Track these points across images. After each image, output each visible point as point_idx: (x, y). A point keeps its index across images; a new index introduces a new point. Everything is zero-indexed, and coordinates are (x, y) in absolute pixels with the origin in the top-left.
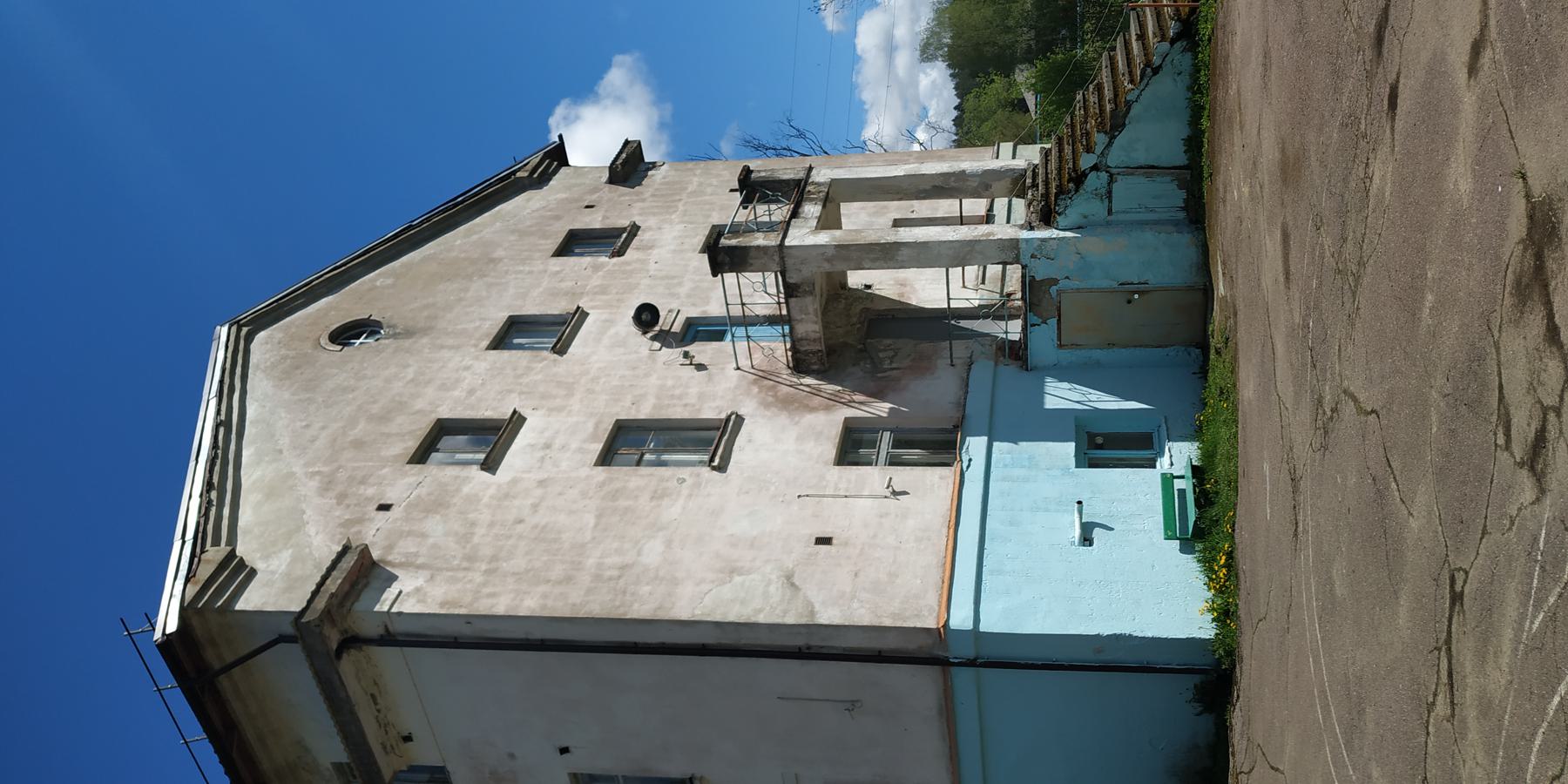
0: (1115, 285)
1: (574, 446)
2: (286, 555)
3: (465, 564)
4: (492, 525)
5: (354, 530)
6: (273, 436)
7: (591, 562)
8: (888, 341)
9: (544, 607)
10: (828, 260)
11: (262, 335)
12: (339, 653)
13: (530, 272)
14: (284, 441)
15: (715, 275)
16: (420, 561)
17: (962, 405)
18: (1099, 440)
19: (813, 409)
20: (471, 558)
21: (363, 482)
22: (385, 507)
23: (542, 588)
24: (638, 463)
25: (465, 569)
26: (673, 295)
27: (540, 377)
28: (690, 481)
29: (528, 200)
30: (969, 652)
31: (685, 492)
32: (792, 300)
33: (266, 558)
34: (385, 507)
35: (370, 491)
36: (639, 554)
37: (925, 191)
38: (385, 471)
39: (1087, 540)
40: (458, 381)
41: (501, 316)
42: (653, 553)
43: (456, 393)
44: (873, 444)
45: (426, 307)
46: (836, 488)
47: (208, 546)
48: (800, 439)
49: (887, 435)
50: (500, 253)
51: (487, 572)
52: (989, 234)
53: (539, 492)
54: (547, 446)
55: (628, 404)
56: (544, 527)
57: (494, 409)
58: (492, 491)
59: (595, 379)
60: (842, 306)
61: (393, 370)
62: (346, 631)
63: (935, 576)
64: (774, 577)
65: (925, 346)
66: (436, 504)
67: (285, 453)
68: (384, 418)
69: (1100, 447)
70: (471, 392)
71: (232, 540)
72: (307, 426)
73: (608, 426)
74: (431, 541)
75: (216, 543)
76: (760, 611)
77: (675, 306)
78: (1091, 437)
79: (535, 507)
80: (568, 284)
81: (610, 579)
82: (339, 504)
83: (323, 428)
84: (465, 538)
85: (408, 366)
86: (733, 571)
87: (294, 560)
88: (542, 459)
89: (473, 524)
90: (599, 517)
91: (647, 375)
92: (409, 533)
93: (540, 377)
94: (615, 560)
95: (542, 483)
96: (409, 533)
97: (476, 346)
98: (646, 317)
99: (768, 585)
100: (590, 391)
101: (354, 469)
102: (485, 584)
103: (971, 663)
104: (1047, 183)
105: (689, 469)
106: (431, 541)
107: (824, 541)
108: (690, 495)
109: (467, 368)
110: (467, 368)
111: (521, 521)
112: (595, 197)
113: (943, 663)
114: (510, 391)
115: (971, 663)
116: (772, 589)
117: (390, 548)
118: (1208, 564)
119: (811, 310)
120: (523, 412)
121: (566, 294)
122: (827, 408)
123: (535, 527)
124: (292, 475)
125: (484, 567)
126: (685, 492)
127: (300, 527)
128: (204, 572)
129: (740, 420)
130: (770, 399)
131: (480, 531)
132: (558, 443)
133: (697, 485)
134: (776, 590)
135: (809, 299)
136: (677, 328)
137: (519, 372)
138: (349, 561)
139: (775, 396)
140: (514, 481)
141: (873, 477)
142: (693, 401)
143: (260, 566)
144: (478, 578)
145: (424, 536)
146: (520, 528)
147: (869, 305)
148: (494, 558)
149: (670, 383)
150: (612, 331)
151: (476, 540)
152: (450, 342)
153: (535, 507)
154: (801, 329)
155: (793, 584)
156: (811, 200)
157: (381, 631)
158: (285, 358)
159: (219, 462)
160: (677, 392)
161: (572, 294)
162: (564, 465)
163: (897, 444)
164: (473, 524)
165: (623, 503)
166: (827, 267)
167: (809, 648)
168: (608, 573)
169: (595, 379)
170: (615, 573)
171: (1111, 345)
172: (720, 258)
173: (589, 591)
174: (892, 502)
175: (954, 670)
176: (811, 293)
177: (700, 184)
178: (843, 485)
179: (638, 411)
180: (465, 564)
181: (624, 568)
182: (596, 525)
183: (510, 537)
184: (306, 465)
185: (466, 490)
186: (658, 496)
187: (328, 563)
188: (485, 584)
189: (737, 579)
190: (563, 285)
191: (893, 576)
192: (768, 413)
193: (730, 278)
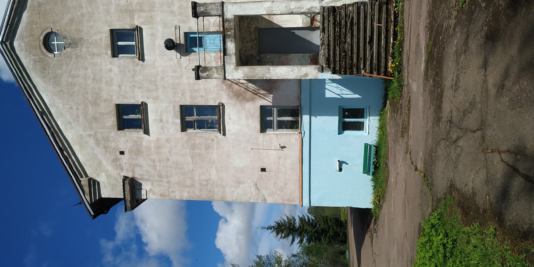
2: (103, 174)
5: (118, 163)
6: (62, 114)
7: (196, 178)
9: (190, 196)
16: (146, 177)
17: (300, 98)
18: (347, 113)
19: (248, 100)
21: (108, 141)
22: (122, 153)
23: (187, 189)
25: (161, 181)
26: (172, 12)
27: (141, 77)
28: (215, 140)
33: (98, 176)
34: (122, 153)
35: (113, 145)
38: (112, 134)
39: (340, 170)
40: (111, 80)
41: (107, 29)
42: (214, 175)
44: (271, 115)
45: (72, 21)
46: (263, 146)
47: (81, 179)
48: (246, 118)
49: (275, 109)
52: (306, 75)
53: (168, 145)
55: (181, 96)
57: (133, 98)
58: (152, 145)
59: (163, 78)
63: (298, 184)
64: (252, 185)
67: (73, 124)
68: (95, 104)
70: (120, 86)
71: (87, 176)
72: (71, 108)
73: (178, 109)
74: (144, 169)
75: (82, 177)
76: (250, 198)
77: (176, 23)
78: (344, 110)
79: (170, 152)
81: (205, 185)
82: (106, 151)
83: (77, 109)
84: (154, 167)
85: (86, 69)
87: (108, 176)
88: (162, 128)
89: (154, 161)
90: (192, 158)
91: (181, 76)
93: (141, 77)
94: (203, 177)
95: (167, 140)
97: (107, 54)
98: (170, 45)
99: (251, 188)
100: (164, 87)
101: (102, 133)
102: (169, 187)
104: (329, 45)
106: (144, 169)
107: (263, 170)
108: (217, 148)
110: (111, 70)
111: (168, 160)
114: (134, 86)
116: (252, 189)
117: (133, 172)
118: (375, 179)
120: (146, 101)
122: (253, 100)
123: (174, 162)
124: (81, 136)
125: (166, 180)
126: (215, 146)
127: (100, 164)
128: (86, 189)
129: (223, 105)
130: (231, 94)
131: (158, 164)
132: (164, 120)
133: (218, 143)
134: (253, 189)
136: (183, 42)
137: (132, 73)
138: (127, 182)
139: (232, 91)
140: (158, 140)
141: (274, 136)
142: (204, 94)
143: (98, 179)
144: (167, 185)
145: (141, 166)
146: (169, 162)
151: (158, 168)
152: (95, 51)
153: (170, 152)
156: (230, 36)
158: (35, 61)
159: (55, 135)
160: (196, 88)
161: (129, 11)
162: (171, 130)
163: (279, 115)
165: (198, 151)
169: (163, 78)
173: (201, 191)
174: (281, 152)
178: (265, 144)
179: (186, 100)
180: (160, 179)
181: (207, 181)
182: (192, 162)
183: (168, 167)
184: (84, 130)
185: (144, 144)
187: (122, 190)
188: (169, 187)
189: (242, 186)
191: (286, 184)
192: (232, 102)
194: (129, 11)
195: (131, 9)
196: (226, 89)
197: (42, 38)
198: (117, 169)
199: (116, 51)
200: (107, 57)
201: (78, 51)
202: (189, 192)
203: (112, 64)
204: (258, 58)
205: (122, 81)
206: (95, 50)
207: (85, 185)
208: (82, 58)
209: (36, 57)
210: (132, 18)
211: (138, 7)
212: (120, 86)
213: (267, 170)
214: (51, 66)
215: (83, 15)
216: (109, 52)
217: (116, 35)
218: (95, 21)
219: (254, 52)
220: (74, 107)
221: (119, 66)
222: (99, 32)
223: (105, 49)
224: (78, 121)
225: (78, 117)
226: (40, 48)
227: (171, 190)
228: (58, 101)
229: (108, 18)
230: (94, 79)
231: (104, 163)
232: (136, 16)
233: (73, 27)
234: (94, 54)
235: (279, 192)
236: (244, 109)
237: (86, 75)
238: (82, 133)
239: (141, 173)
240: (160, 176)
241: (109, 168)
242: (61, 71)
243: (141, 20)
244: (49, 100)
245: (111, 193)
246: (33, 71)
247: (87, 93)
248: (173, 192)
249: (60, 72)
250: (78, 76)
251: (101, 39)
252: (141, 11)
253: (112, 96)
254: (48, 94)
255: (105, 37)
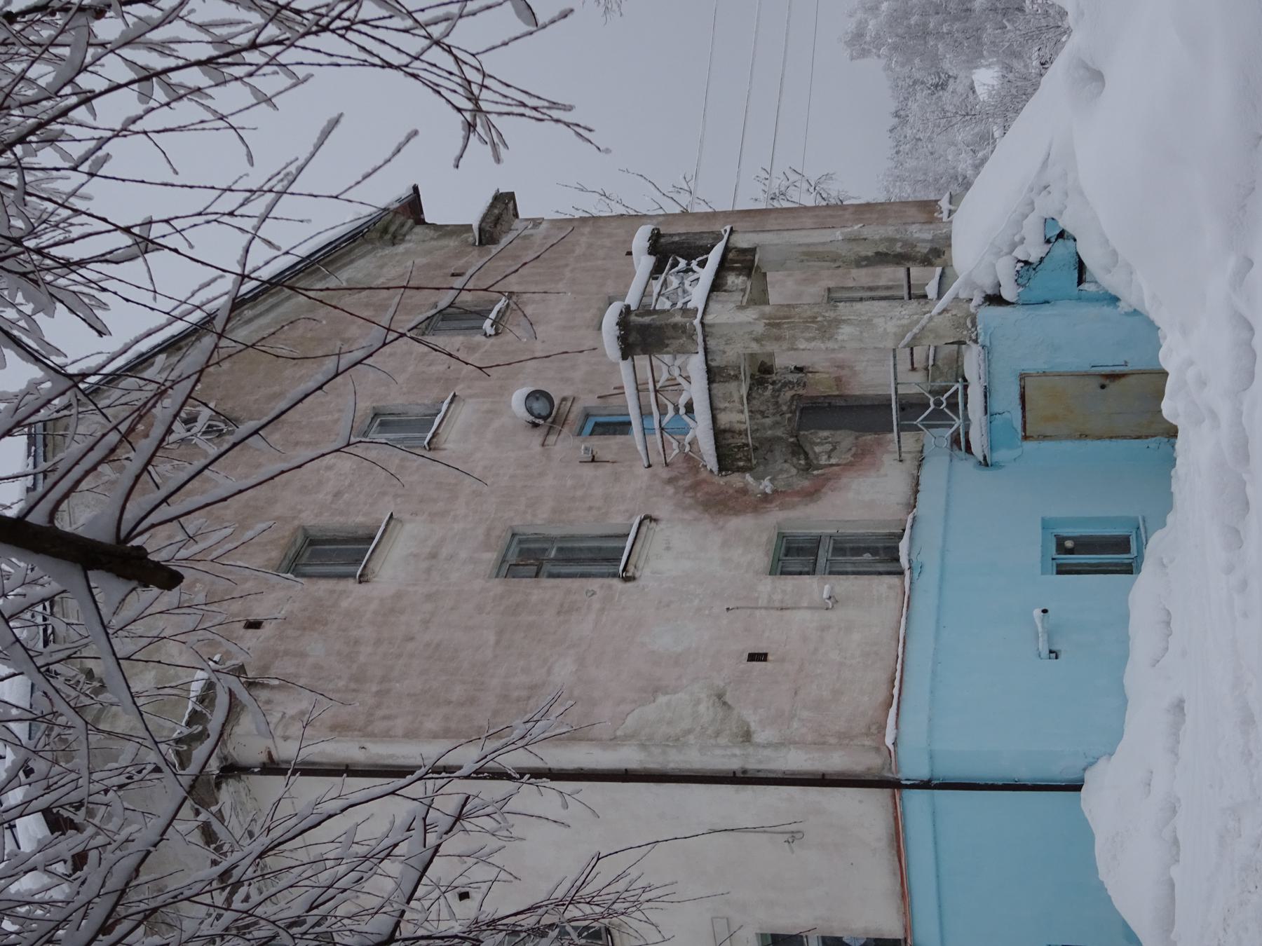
0: (1085, 367)
1: (463, 555)
3: (353, 686)
4: (378, 642)
8: (825, 433)
10: (757, 340)
12: (218, 786)
15: (624, 357)
18: (1069, 544)
20: (359, 678)
22: (254, 625)
24: (537, 576)
29: (381, 267)
30: (923, 773)
31: (596, 606)
32: (715, 385)
34: (254, 625)
36: (549, 672)
37: (867, 258)
42: (564, 671)
43: (321, 496)
48: (725, 544)
51: (378, 693)
54: (433, 556)
56: (438, 645)
58: (374, 606)
60: (768, 393)
62: (225, 758)
64: (703, 696)
65: (869, 438)
66: (314, 621)
69: (1070, 551)
70: (337, 495)
77: (568, 392)
79: (426, 623)
81: (518, 700)
86: (657, 691)
88: (428, 571)
89: (357, 642)
90: (500, 633)
91: (542, 474)
92: (286, 653)
95: (429, 597)
96: (286, 653)
103: (925, 785)
105: (599, 580)
108: (602, 610)
111: (412, 639)
112: (461, 262)
113: (894, 785)
114: (384, 494)
115: (925, 785)
117: (266, 668)
119: (736, 398)
121: (438, 380)
123: (428, 645)
125: (374, 688)
126: (596, 606)
130: (688, 501)
132: (445, 552)
135: (732, 386)
140: (398, 596)
145: (303, 655)
146: (410, 646)
147: (801, 392)
148: (384, 679)
149: (569, 483)
150: (496, 424)
151: (362, 659)
152: (307, 437)
153: (426, 623)
154: (725, 419)
155: (725, 703)
156: (733, 269)
157: (263, 758)
160: (579, 493)
164: (357, 642)
166: (755, 347)
167: (745, 772)
168: (516, 694)
170: (524, 693)
171: (1083, 436)
172: (631, 339)
173: (496, 713)
175: (906, 792)
176: (736, 377)
177: (590, 246)
180: (353, 686)
181: (533, 688)
182: (497, 643)
183: (399, 656)
185: (344, 604)
186: (565, 610)
188: (378, 706)
189: (662, 699)
190: (434, 369)
192: (686, 517)
193: (642, 361)
196: (676, 493)
202: (446, 718)
204: (791, 440)
205: (351, 485)
212: (337, 495)
213: (770, 657)
219: (779, 432)
227: (380, 713)
235: (805, 714)
236: (722, 528)
239: (292, 670)
240: (359, 678)
248: (385, 718)
251: (336, 421)
253: (300, 511)
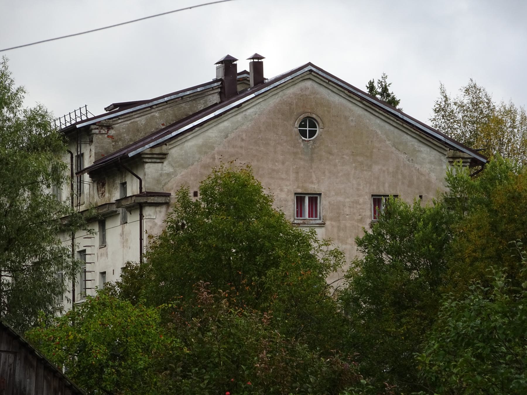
2: (171, 170)
11: (309, 83)
13: (358, 189)
14: (231, 136)
29: (431, 162)
33: (169, 163)
50: (376, 168)
61: (281, 157)
72: (242, 140)
80: (347, 210)
83: (241, 147)
85: (283, 163)
87: (169, 175)
97: (298, 187)
109: (281, 190)
110: (281, 190)
128: (157, 150)
143: (166, 163)
152: (301, 175)
158: (291, 104)
184: (219, 153)
194: (339, 216)
195: (341, 218)
197: (314, 116)
198: (177, 186)
199: (300, 199)
200: (295, 187)
201: (301, 156)
203: (288, 192)
206: (302, 175)
207: (161, 149)
208: (293, 159)
209: (294, 106)
210: (331, 219)
211: (342, 226)
214: (285, 122)
215: (335, 165)
216: (299, 191)
217: (314, 199)
218: (330, 178)
220: (243, 144)
221: (286, 200)
222: (319, 182)
223: (303, 187)
224: (228, 146)
225: (233, 147)
226: (304, 113)
228: (250, 125)
229: (333, 193)
230: (273, 170)
231: (184, 172)
232: (334, 223)
233: (324, 154)
234: (297, 173)
237: (276, 161)
238: (216, 149)
241: (179, 177)
242: (280, 133)
243: (329, 228)
244: (250, 115)
245: (150, 176)
246: (281, 101)
247: (258, 161)
249: (280, 132)
250: (275, 152)
252: (339, 229)
254: (257, 115)
255: (314, 188)
